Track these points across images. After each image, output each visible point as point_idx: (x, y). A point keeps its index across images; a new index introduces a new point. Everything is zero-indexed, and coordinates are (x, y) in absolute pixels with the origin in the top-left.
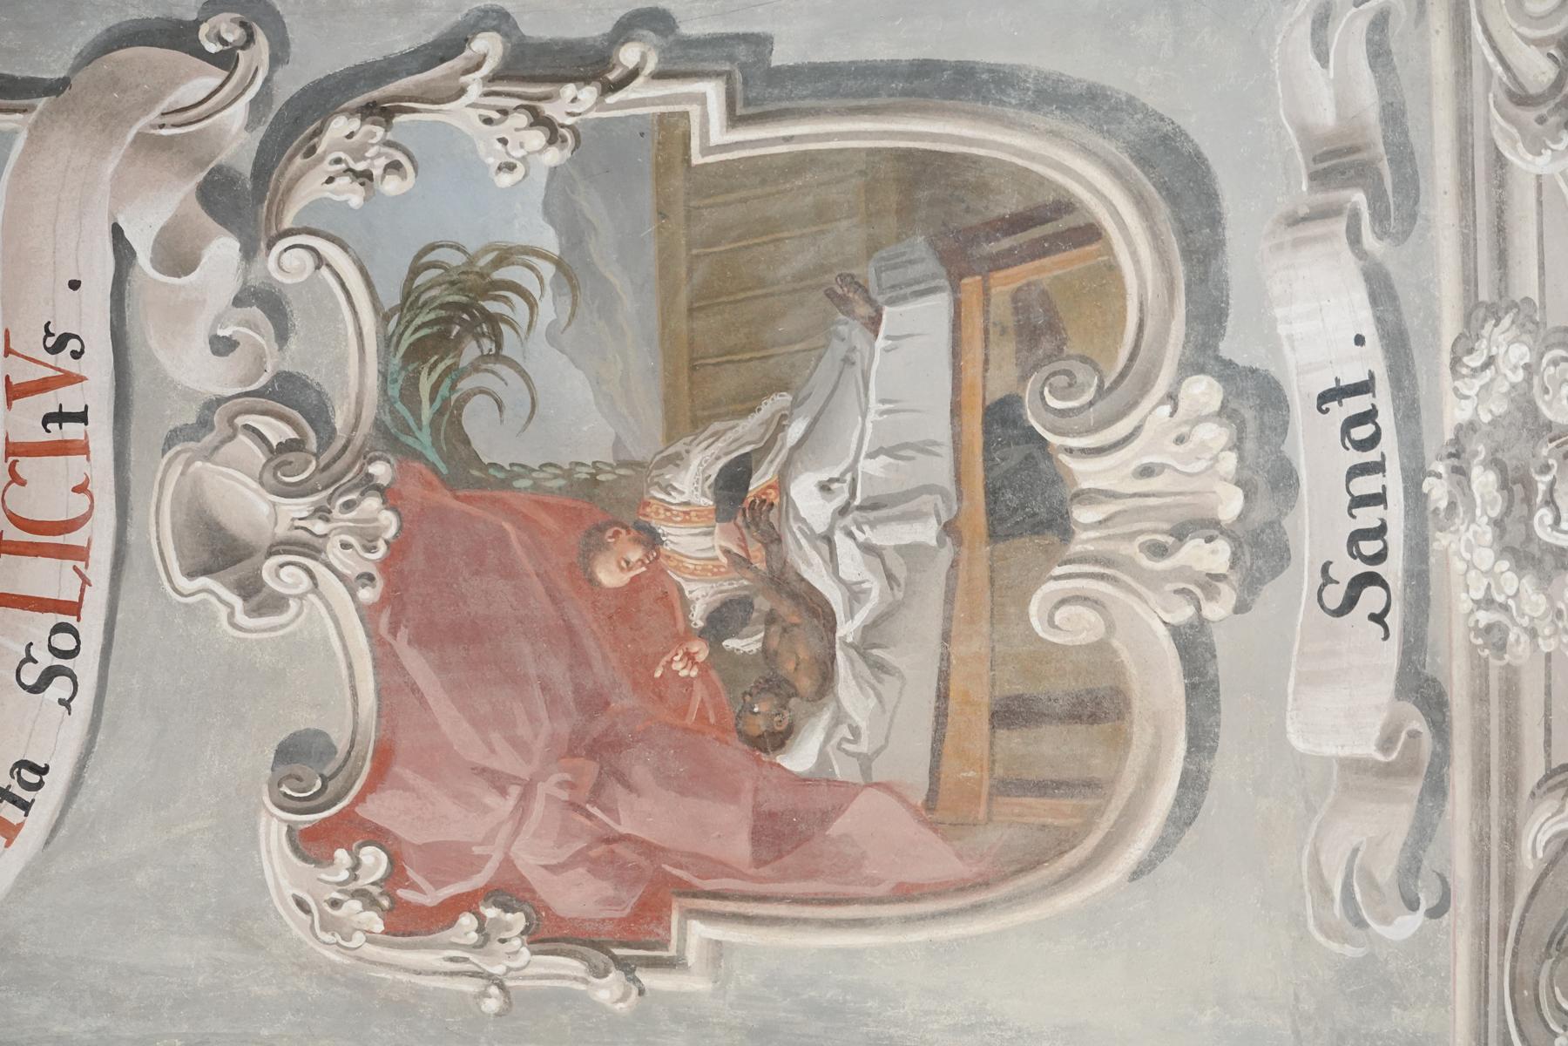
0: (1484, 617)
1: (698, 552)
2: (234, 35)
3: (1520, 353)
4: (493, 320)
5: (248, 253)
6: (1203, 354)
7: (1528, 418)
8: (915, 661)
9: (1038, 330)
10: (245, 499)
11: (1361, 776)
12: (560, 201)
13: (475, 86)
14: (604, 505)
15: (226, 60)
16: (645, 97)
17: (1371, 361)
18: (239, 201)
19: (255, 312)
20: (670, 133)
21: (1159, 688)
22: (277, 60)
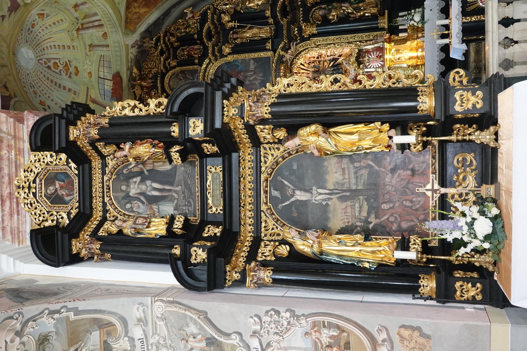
0: (21, 186)
2: (17, 316)
3: (158, 337)
4: (48, 339)
5: (20, 339)
7: (158, 342)
9: (109, 334)
12: (55, 326)
13: (45, 316)
15: (17, 319)
16: (65, 314)
17: (143, 337)
18: (19, 334)
19: (22, 345)
20: (68, 318)
22: (23, 317)
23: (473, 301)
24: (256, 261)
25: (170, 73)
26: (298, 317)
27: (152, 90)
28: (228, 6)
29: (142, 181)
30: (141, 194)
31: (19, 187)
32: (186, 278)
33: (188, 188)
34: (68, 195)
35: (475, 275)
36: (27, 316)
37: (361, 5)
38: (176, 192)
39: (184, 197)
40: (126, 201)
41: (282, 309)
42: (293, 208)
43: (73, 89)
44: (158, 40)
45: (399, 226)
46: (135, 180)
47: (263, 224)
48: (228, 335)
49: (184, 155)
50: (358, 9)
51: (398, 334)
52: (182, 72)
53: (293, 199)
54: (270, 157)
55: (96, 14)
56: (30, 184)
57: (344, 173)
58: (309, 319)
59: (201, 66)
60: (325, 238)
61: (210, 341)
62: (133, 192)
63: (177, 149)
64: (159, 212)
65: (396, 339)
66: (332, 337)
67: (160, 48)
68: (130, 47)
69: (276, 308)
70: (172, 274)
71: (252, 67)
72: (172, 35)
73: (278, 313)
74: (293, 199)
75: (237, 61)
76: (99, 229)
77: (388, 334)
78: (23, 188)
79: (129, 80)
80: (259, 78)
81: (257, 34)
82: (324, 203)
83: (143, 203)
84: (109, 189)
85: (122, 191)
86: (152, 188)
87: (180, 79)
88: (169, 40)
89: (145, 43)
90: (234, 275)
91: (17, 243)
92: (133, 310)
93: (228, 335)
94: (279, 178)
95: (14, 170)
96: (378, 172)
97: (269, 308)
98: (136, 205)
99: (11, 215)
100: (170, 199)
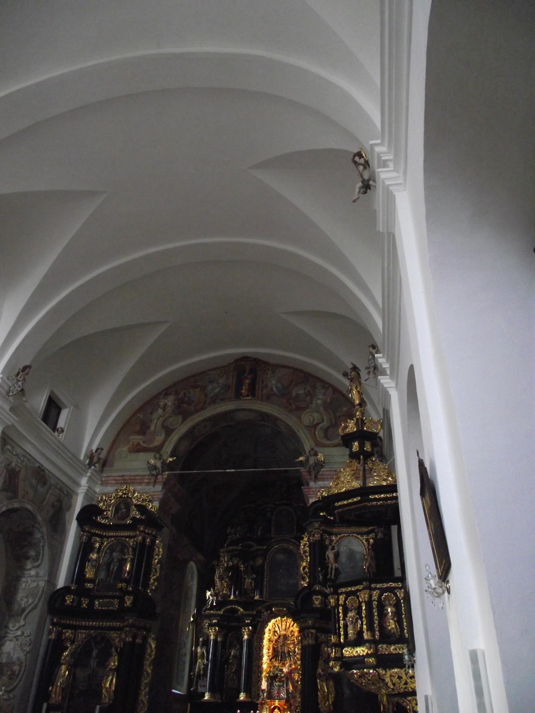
47: (84, 631)
49: (121, 589)
62: (115, 554)
86: (114, 567)
95: (138, 481)
99: (115, 480)
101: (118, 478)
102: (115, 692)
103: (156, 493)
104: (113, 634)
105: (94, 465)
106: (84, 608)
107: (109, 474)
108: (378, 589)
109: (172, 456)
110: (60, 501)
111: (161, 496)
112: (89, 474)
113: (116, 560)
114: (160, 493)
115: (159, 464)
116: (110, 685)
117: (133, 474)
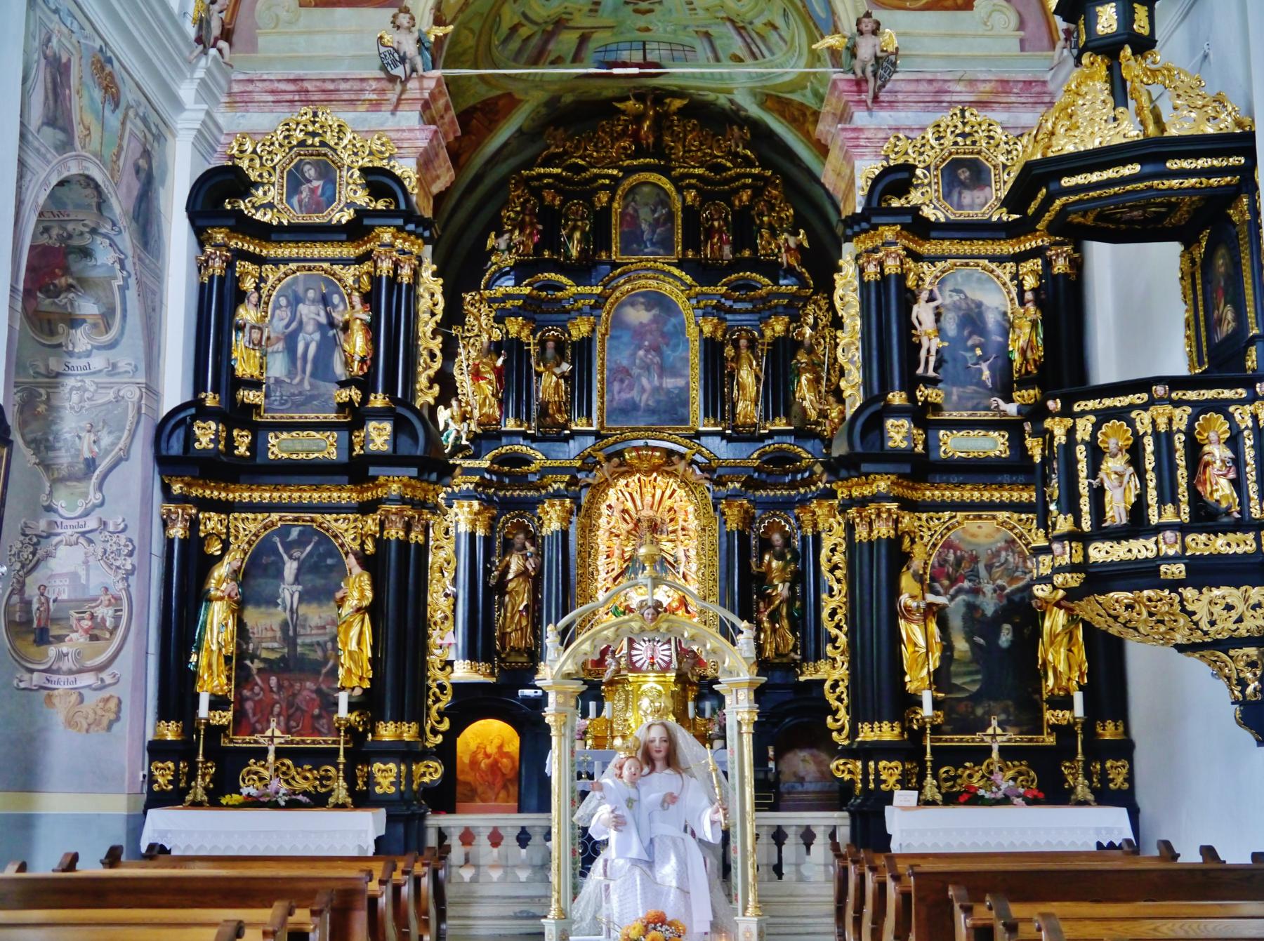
1: (62, 281)
6: (94, 347)
7: (86, 390)
8: (52, 309)
9: (95, 326)
10: (55, 232)
11: (47, 366)
12: (103, 265)
14: (66, 271)
16: (119, 274)
20: (115, 278)
21: (55, 341)
23: (151, 779)
24: (198, 512)
25: (668, 186)
26: (126, 579)
27: (633, 142)
28: (808, 331)
29: (320, 326)
30: (301, 323)
31: (315, 114)
32: (173, 422)
33: (306, 401)
34: (300, 202)
35: (182, 785)
36: (117, 239)
37: (785, 623)
38: (302, 381)
39: (293, 395)
40: (291, 298)
41: (135, 559)
42: (273, 558)
43: (601, 8)
44: (748, 162)
45: (248, 699)
46: (322, 313)
47: (251, 516)
48: (100, 487)
50: (774, 617)
51: (111, 697)
52: (671, 216)
53: (285, 557)
54: (344, 526)
55: (773, 54)
56: (318, 135)
57: (319, 628)
58: (124, 595)
59: (679, 265)
60: (229, 606)
61: (91, 464)
63: (354, 397)
64: (273, 352)
65: (105, 694)
66: (103, 620)
67: (729, 164)
68: (730, 96)
69: (136, 552)
70: (178, 403)
71: (670, 383)
72: (757, 193)
73: (131, 554)
74: (285, 557)
75: (687, 349)
76: (244, 260)
77: (110, 685)
78: (314, 123)
79: (656, 88)
80: (645, 397)
81: (744, 395)
82: (279, 601)
83: (287, 326)
84: (310, 270)
85: (307, 290)
86: (309, 342)
87: (654, 211)
88: (745, 186)
89: (741, 129)
90: (178, 486)
91: (227, 100)
92: (128, 356)
93: (100, 487)
94: (316, 539)
95: (346, 97)
96: (319, 673)
97: (136, 543)
98: (284, 314)
99: (273, 92)
100: (291, 373)
101: (283, 86)
102: (374, 661)
103: (406, 135)
104: (336, 520)
105: (214, 46)
106: (242, 457)
107: (252, 74)
108: (1188, 403)
109: (438, 21)
110: (146, 154)
111: (424, 144)
112: (200, 73)
113: (310, 327)
114: (418, 134)
115: (410, 48)
116: (359, 643)
117: (330, 74)
